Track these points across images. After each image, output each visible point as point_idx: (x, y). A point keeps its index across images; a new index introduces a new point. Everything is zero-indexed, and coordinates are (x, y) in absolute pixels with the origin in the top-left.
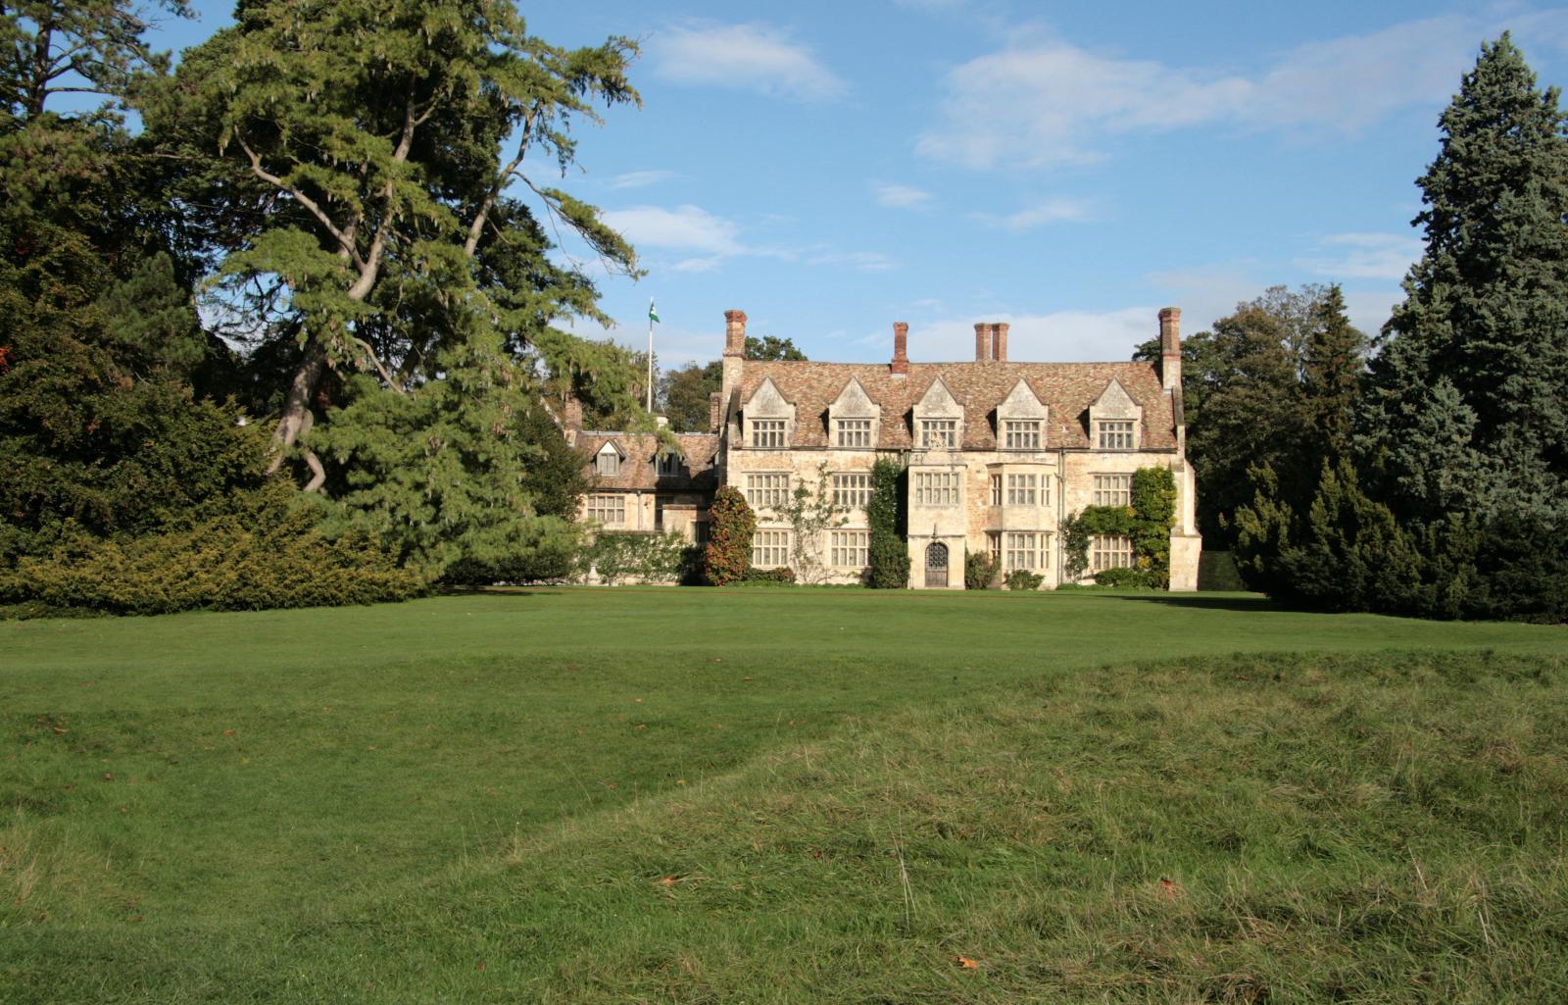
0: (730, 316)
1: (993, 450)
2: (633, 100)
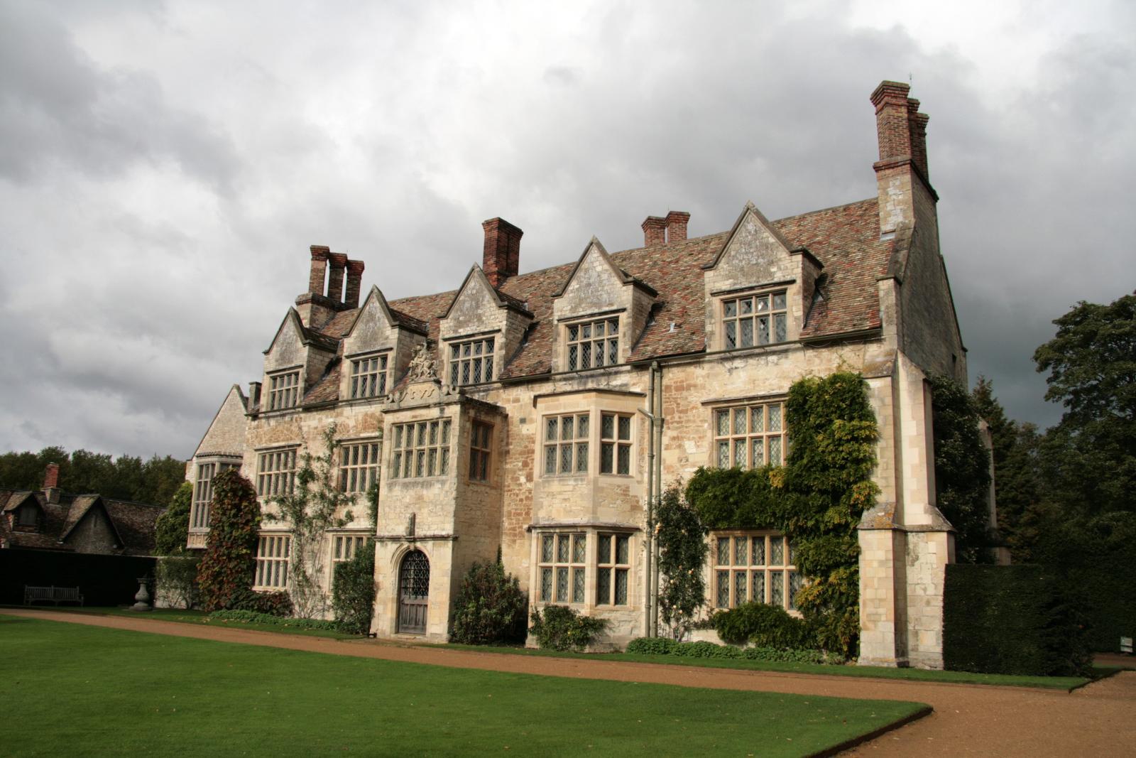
1: (546, 377)
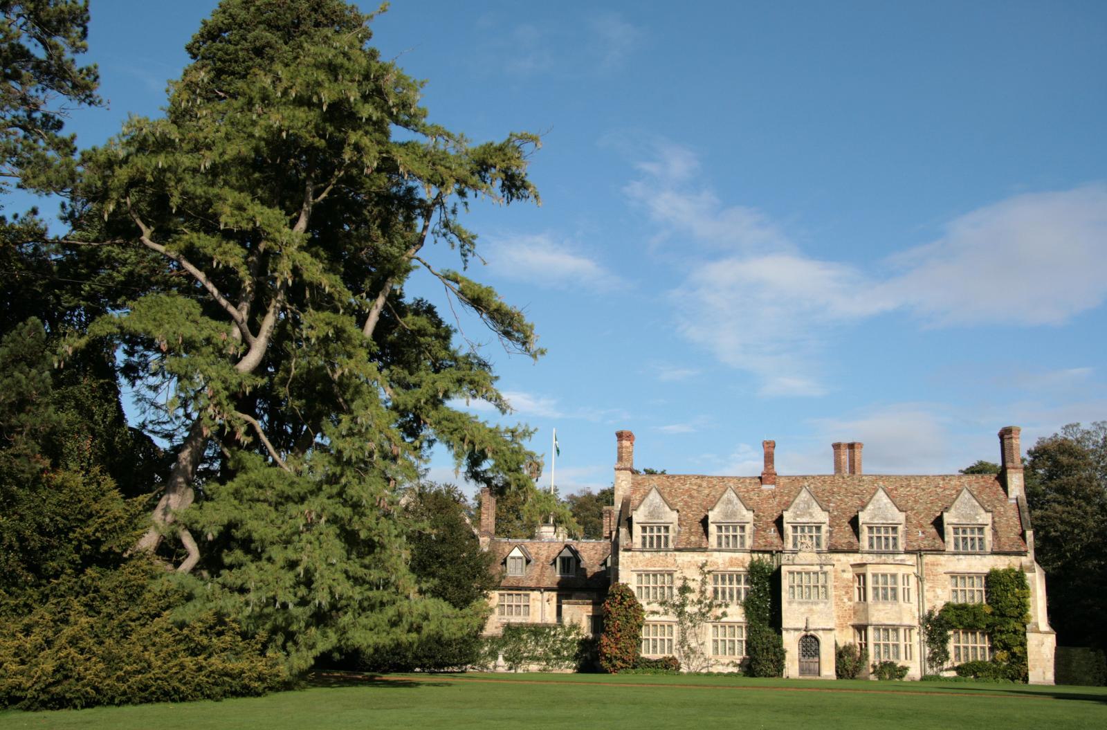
0: (620, 436)
1: (856, 552)
2: (532, 197)
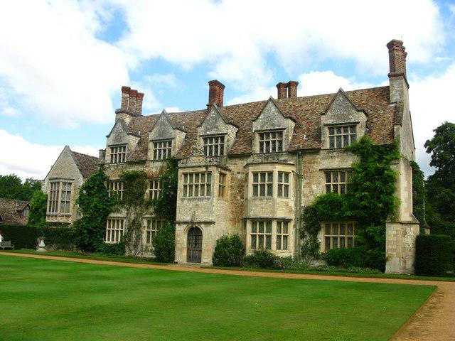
1: (248, 155)
